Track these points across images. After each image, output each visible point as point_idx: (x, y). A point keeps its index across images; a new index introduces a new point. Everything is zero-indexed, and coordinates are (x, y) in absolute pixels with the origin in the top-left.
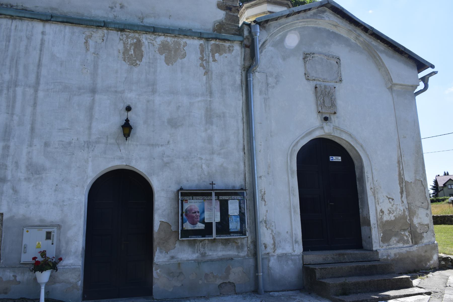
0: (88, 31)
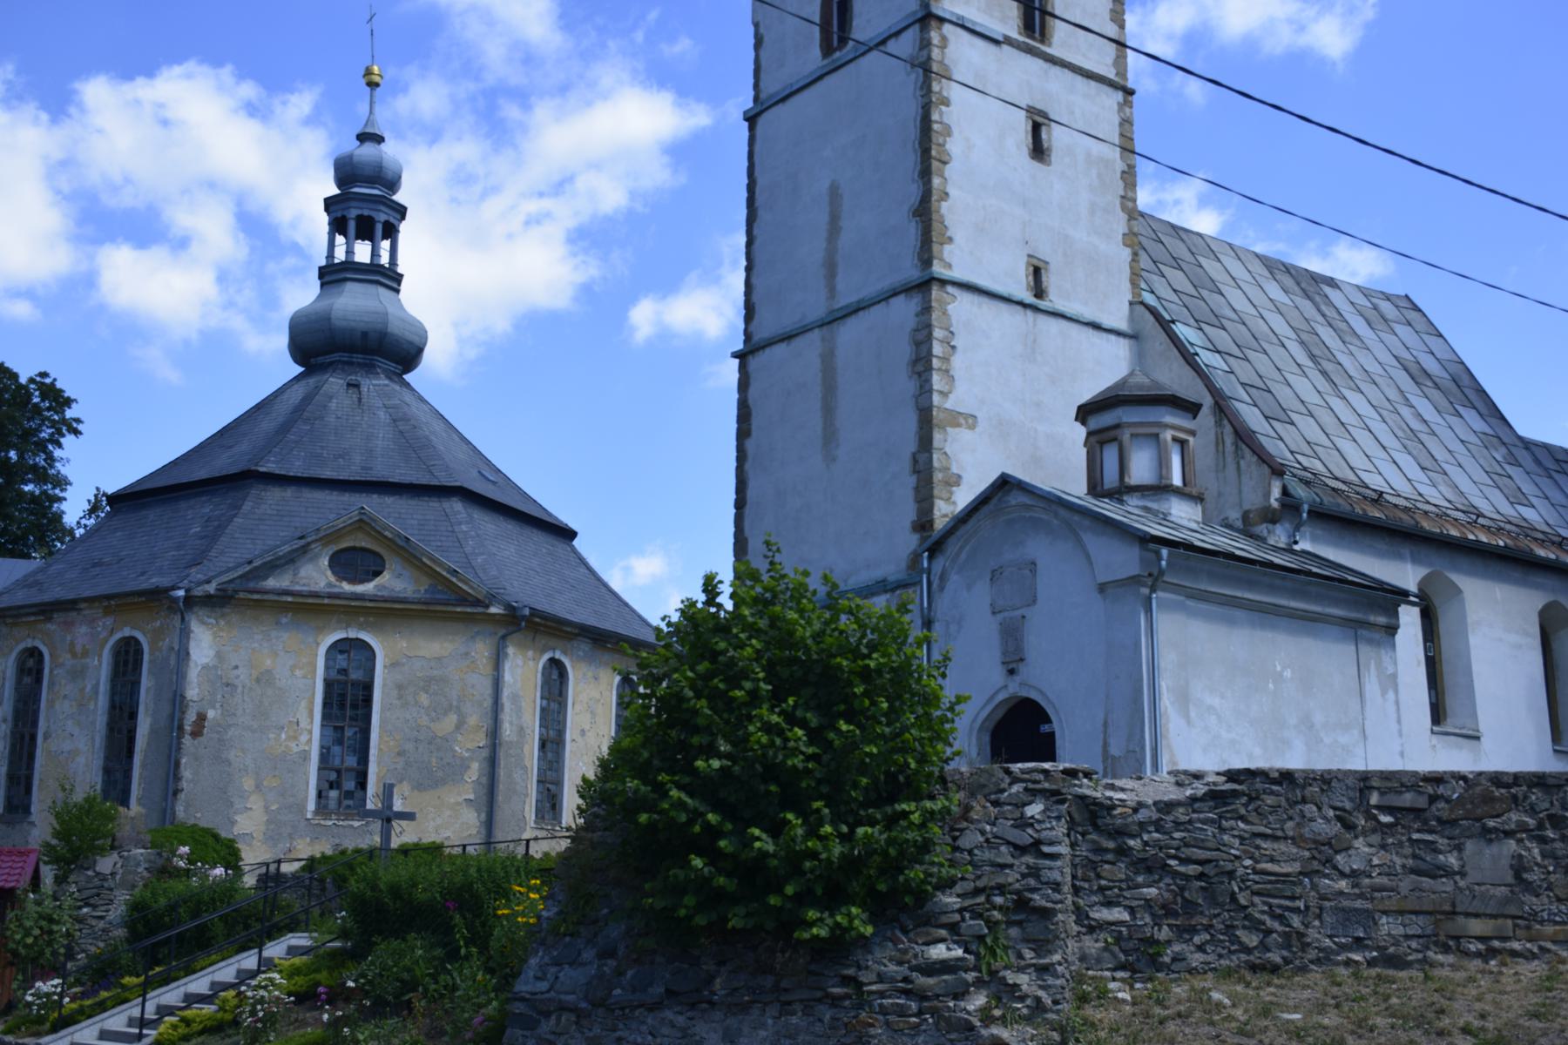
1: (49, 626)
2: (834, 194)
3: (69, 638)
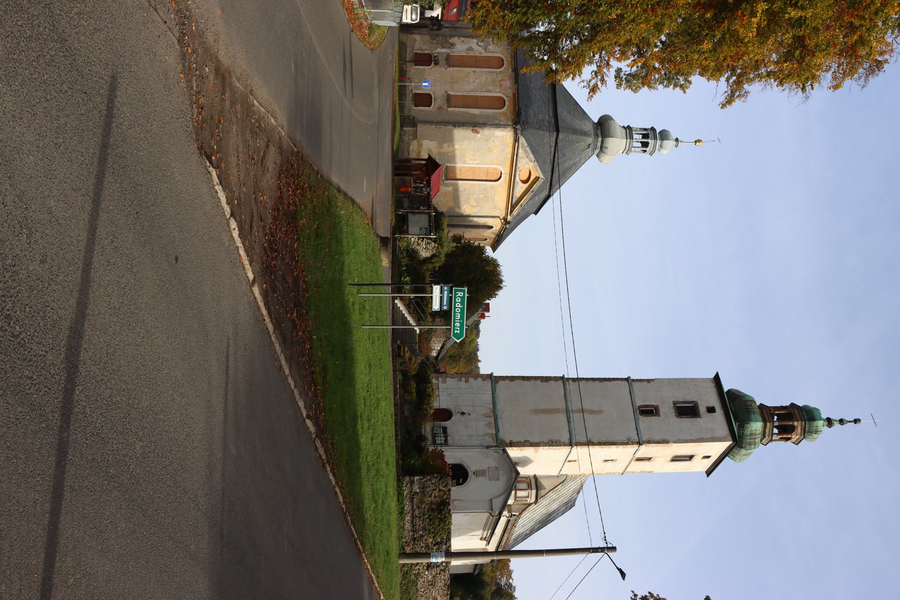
0: (492, 404)
1: (511, 70)
2: (600, 412)
3: (506, 78)
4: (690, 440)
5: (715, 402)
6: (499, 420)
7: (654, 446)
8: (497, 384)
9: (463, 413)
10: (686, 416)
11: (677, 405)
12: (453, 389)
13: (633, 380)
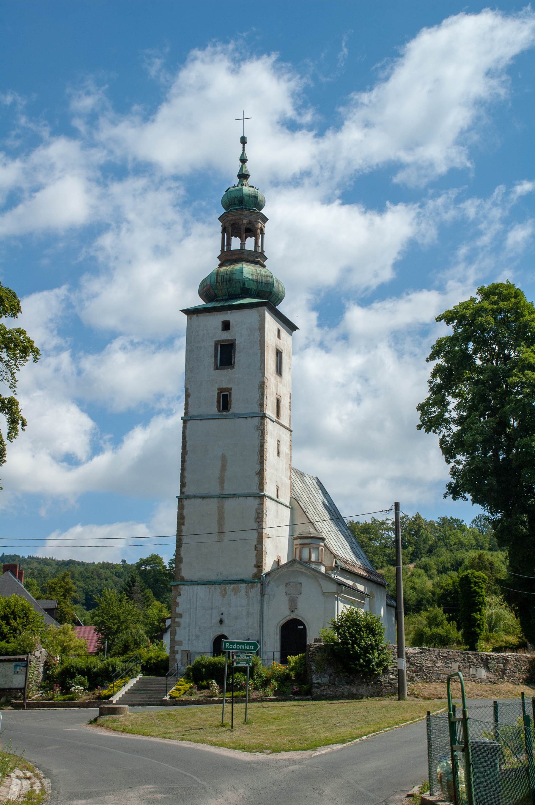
0: (210, 586)
2: (224, 457)
4: (261, 356)
5: (217, 319)
6: (230, 578)
7: (267, 398)
8: (185, 579)
9: (221, 621)
10: (233, 357)
11: (219, 365)
12: (189, 632)
13: (186, 414)
